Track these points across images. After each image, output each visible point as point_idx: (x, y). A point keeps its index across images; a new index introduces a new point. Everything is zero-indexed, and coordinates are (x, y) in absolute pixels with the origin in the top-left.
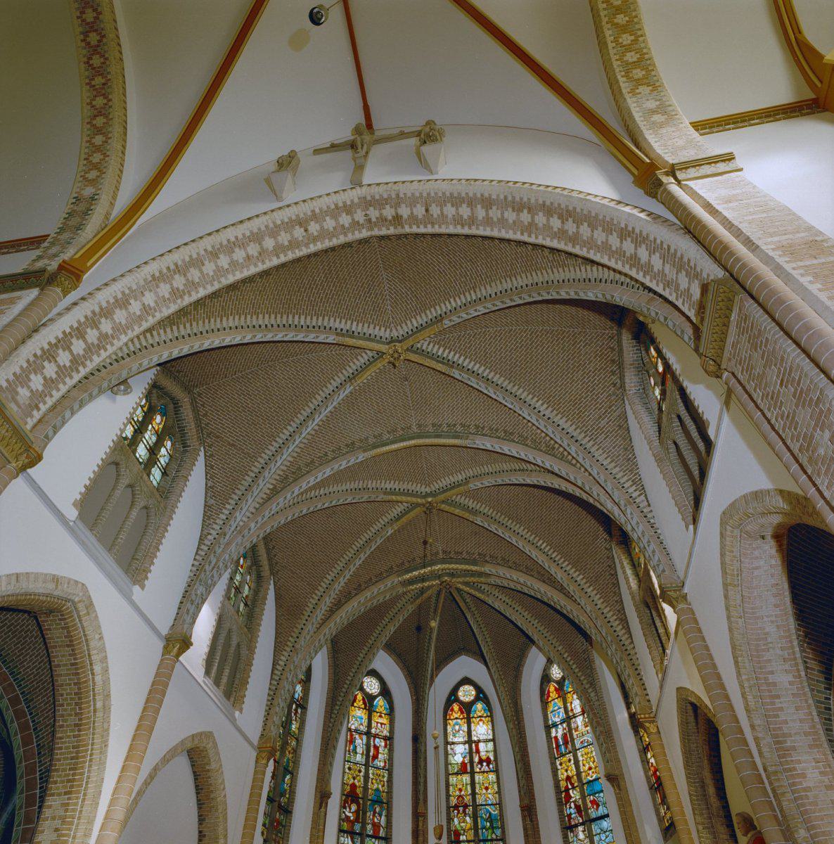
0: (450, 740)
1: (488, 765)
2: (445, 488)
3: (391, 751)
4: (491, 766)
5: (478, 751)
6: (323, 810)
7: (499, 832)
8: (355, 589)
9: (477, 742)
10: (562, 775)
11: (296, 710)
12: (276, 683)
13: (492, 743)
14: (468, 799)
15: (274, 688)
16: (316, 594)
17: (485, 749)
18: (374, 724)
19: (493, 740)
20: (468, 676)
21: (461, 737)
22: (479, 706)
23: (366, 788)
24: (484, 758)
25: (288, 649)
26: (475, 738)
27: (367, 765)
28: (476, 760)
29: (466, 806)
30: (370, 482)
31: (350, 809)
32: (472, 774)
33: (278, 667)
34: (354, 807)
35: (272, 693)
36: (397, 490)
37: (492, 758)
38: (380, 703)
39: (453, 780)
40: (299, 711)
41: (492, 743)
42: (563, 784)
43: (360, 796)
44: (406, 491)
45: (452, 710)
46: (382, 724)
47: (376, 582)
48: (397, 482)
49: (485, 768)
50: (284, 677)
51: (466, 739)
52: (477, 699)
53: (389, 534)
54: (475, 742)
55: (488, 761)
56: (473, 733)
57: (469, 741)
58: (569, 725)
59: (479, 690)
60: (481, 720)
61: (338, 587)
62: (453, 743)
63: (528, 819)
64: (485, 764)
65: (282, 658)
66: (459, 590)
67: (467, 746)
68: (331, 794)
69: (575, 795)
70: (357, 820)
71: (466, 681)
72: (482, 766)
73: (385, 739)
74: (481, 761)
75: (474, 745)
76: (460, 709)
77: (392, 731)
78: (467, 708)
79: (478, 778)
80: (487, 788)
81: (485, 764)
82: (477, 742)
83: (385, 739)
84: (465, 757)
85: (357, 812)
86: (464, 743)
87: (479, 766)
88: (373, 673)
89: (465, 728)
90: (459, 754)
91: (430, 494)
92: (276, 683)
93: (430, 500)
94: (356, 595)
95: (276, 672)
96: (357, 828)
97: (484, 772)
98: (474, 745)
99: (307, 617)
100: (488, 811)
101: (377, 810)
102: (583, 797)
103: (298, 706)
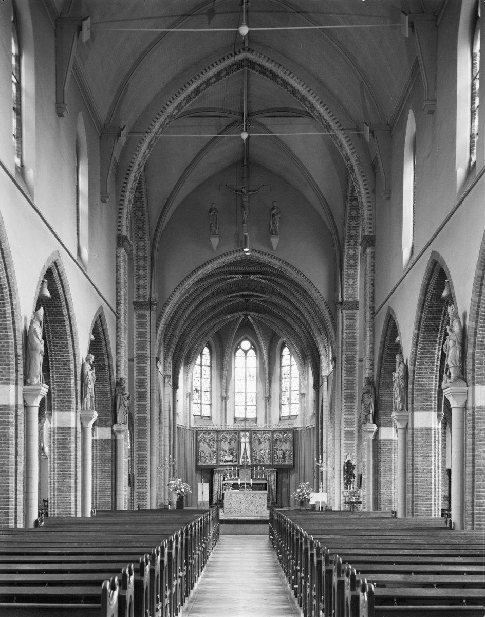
3: (211, 371)
7: (255, 403)
10: (283, 386)
14: (243, 391)
23: (201, 387)
24: (251, 374)
26: (247, 366)
27: (201, 377)
28: (248, 375)
32: (246, 380)
42: (283, 389)
49: (251, 378)
57: (246, 367)
58: (290, 367)
63: (267, 402)
69: (288, 394)
71: (246, 339)
74: (250, 376)
78: (246, 352)
79: (248, 382)
89: (244, 360)
102: (290, 396)
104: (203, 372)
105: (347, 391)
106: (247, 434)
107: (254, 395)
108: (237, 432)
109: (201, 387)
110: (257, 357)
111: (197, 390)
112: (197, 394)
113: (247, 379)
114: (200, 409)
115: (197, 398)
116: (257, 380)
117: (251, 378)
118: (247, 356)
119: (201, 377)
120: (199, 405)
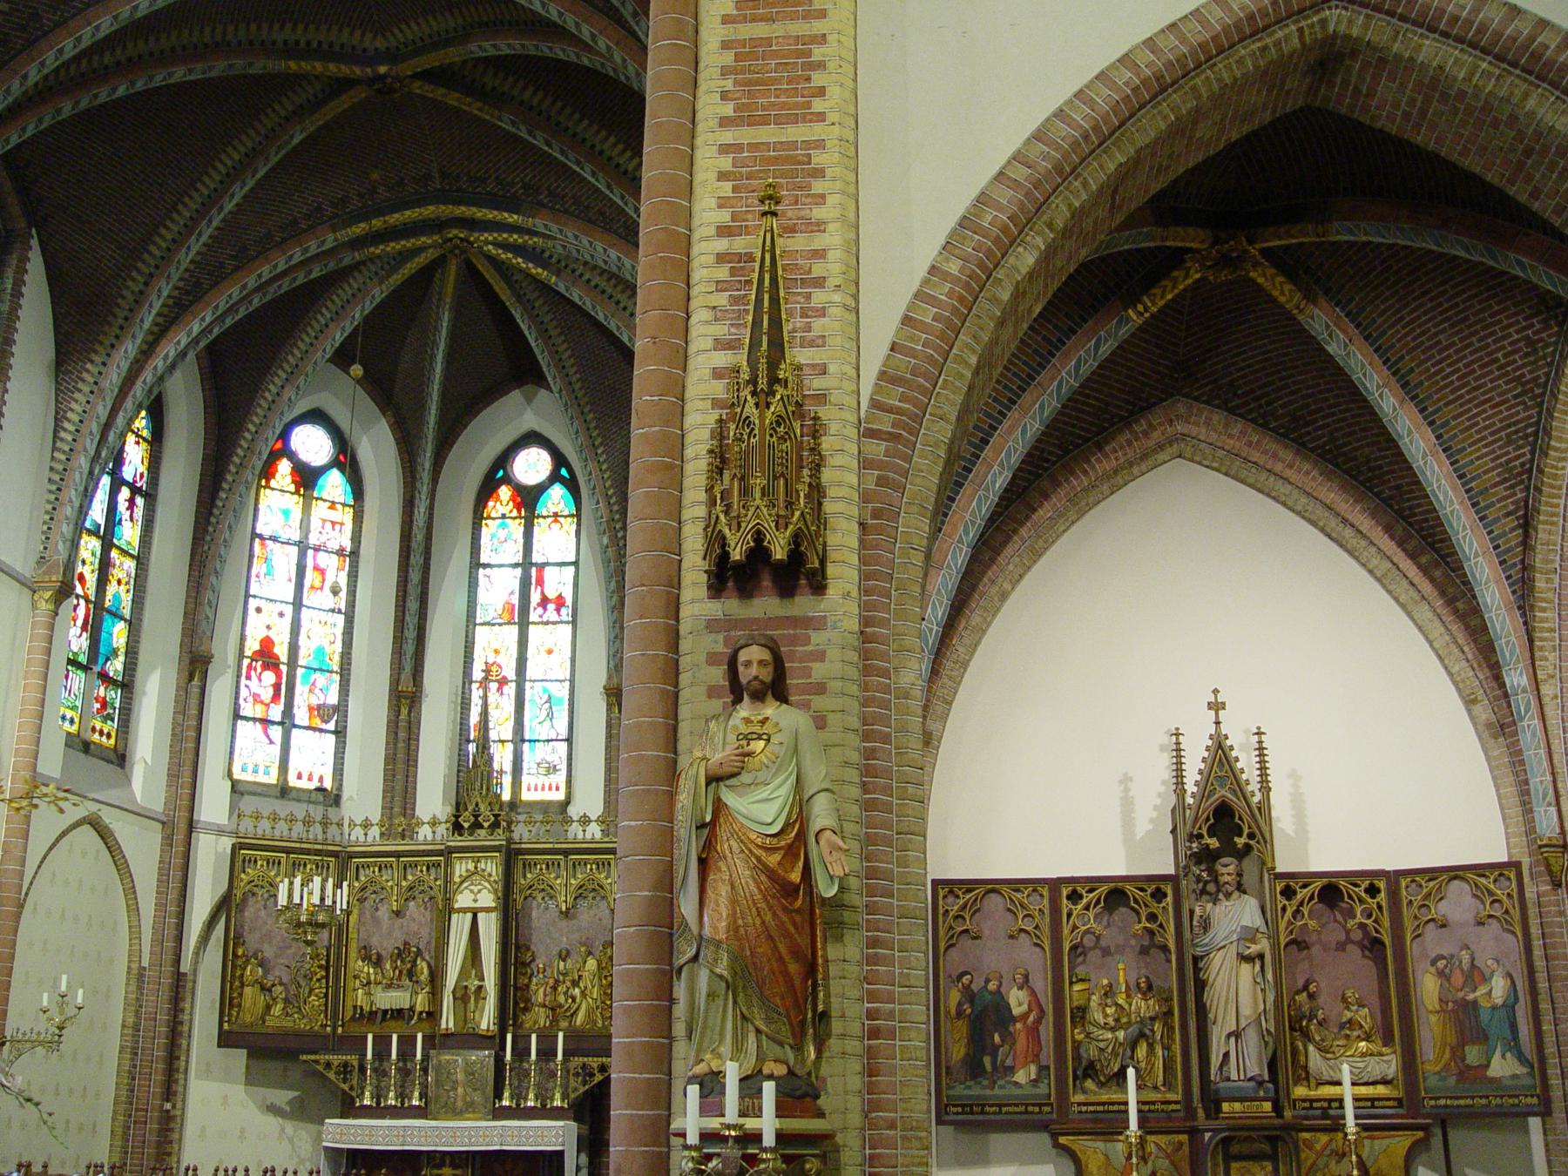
0: (484, 559)
1: (558, 610)
2: (420, 44)
4: (564, 611)
5: (540, 582)
6: (196, 682)
8: (232, 257)
9: (541, 567)
11: (132, 504)
12: (63, 457)
13: (572, 568)
14: (510, 671)
15: (60, 467)
16: (139, 271)
17: (558, 582)
18: (315, 523)
19: (576, 564)
20: (538, 429)
21: (512, 551)
22: (558, 493)
23: (294, 649)
24: (551, 594)
25: (86, 389)
26: (537, 558)
27: (298, 604)
28: (535, 597)
29: (503, 682)
30: (231, 29)
31: (260, 680)
33: (66, 425)
34: (270, 677)
35: (57, 477)
36: (303, 44)
37: (569, 602)
38: (334, 485)
39: (481, 634)
40: (140, 501)
41: (572, 568)
43: (284, 658)
44: (325, 47)
45: (498, 499)
46: (334, 523)
47: (284, 240)
48: (301, 27)
49: (551, 614)
50: (79, 447)
51: (519, 558)
52: (554, 478)
53: (296, 141)
54: (536, 564)
55: (560, 602)
56: (536, 546)
57: (526, 563)
59: (559, 460)
60: (556, 521)
61: (185, 258)
62: (486, 566)
64: (551, 607)
65: (74, 405)
66: (491, 259)
67: (519, 571)
68: (212, 657)
70: (276, 698)
72: (545, 609)
73: (340, 552)
74: (544, 602)
75: (534, 570)
76: (513, 499)
77: (356, 537)
78: (528, 499)
80: (550, 652)
81: (551, 607)
82: (541, 567)
83: (340, 552)
84: (512, 593)
85: (277, 687)
86: (516, 565)
87: (540, 610)
88: (317, 416)
90: (497, 589)
91: (392, 57)
92: (63, 457)
93: (382, 69)
94: (237, 269)
95: (63, 434)
96: (276, 712)
97: (547, 623)
98: (534, 570)
99: (121, 321)
100: (545, 690)
101: (319, 685)
103: (135, 490)
104: (311, 577)
105: (746, 135)
106: (492, 867)
107: (562, 692)
108: (448, 852)
109: (294, 649)
110: (578, 515)
111: (266, 655)
112: (270, 677)
113: (533, 617)
114: (276, 750)
115: (267, 694)
116: (574, 622)
117: (551, 614)
118: (541, 509)
119: (298, 604)
120: (276, 732)
